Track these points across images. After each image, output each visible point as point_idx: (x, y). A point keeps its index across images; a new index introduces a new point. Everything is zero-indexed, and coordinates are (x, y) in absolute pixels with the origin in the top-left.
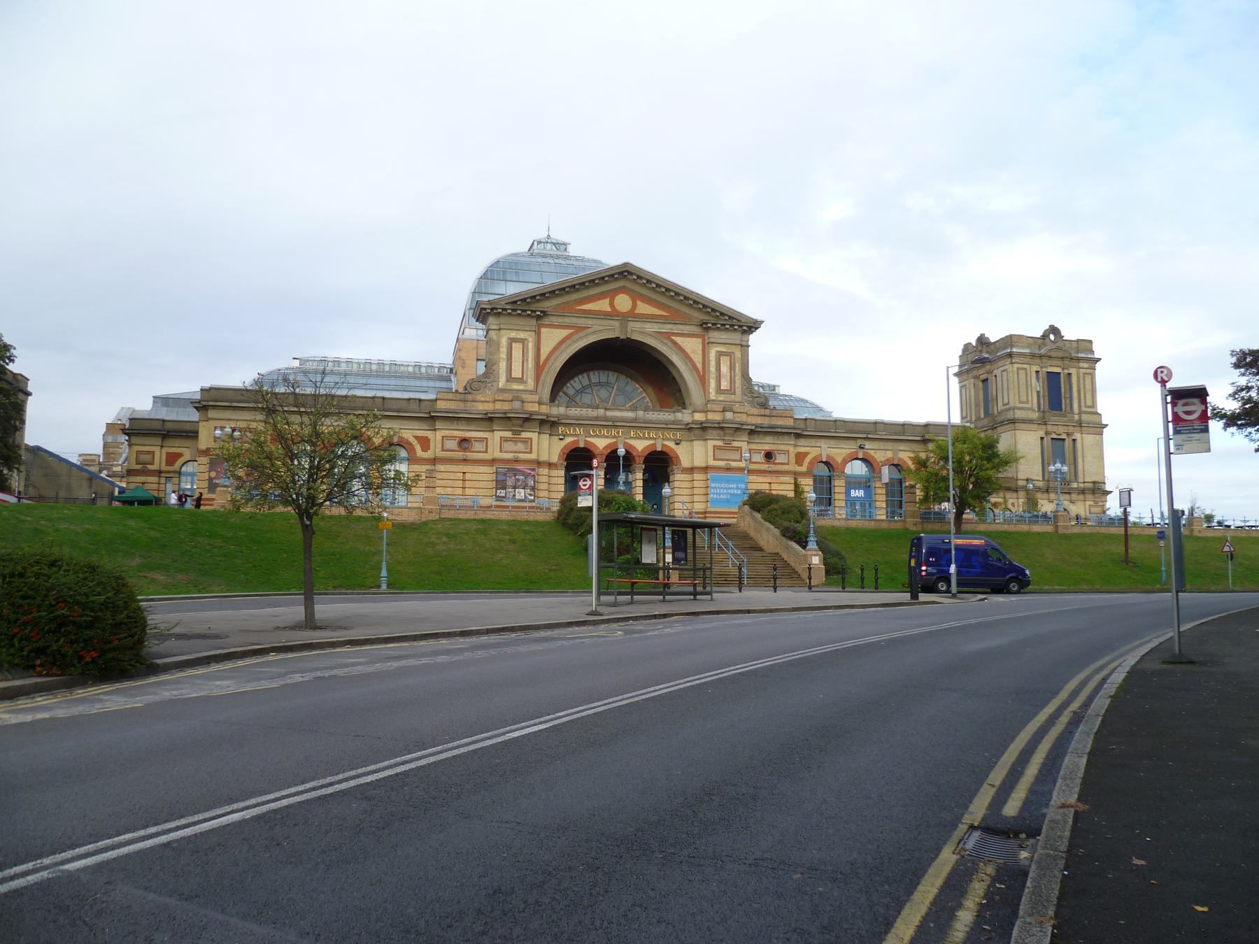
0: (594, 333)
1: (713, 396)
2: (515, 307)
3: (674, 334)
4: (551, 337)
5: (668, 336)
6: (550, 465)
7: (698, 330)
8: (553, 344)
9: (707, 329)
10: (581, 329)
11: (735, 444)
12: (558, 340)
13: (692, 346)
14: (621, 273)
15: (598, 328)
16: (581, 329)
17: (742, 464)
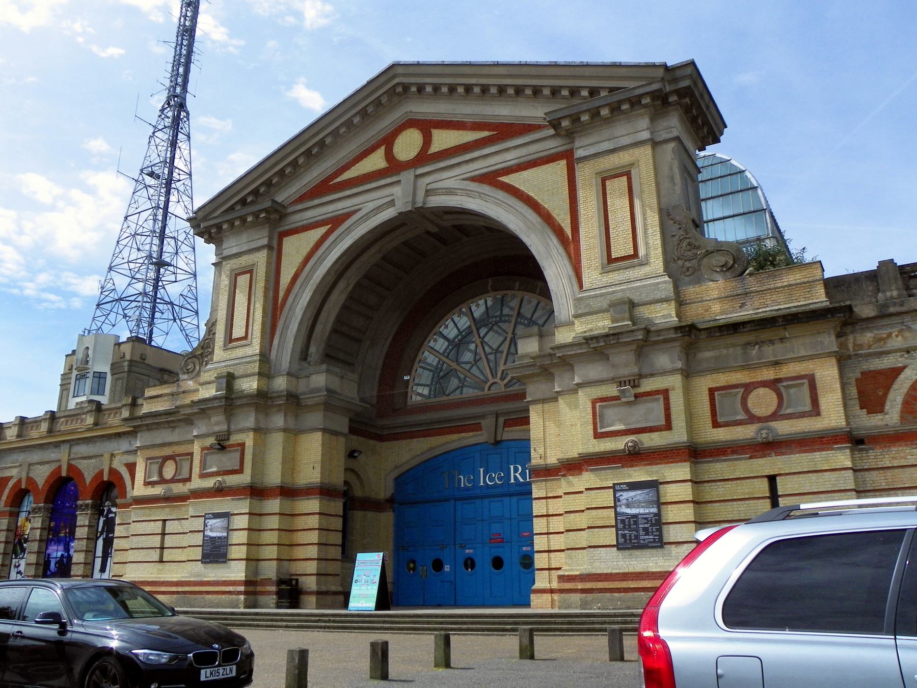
0: (367, 217)
1: (592, 275)
2: (229, 217)
3: (508, 171)
4: (295, 249)
5: (490, 179)
6: (288, 492)
7: (554, 145)
8: (300, 259)
9: (570, 135)
10: (336, 221)
11: (648, 385)
12: (310, 256)
13: (546, 183)
14: (392, 92)
15: (371, 206)
16: (336, 221)
17: (678, 435)
